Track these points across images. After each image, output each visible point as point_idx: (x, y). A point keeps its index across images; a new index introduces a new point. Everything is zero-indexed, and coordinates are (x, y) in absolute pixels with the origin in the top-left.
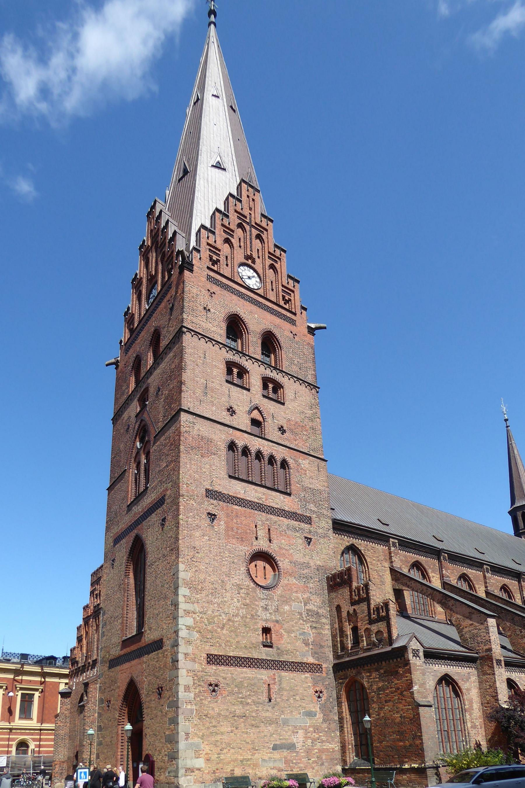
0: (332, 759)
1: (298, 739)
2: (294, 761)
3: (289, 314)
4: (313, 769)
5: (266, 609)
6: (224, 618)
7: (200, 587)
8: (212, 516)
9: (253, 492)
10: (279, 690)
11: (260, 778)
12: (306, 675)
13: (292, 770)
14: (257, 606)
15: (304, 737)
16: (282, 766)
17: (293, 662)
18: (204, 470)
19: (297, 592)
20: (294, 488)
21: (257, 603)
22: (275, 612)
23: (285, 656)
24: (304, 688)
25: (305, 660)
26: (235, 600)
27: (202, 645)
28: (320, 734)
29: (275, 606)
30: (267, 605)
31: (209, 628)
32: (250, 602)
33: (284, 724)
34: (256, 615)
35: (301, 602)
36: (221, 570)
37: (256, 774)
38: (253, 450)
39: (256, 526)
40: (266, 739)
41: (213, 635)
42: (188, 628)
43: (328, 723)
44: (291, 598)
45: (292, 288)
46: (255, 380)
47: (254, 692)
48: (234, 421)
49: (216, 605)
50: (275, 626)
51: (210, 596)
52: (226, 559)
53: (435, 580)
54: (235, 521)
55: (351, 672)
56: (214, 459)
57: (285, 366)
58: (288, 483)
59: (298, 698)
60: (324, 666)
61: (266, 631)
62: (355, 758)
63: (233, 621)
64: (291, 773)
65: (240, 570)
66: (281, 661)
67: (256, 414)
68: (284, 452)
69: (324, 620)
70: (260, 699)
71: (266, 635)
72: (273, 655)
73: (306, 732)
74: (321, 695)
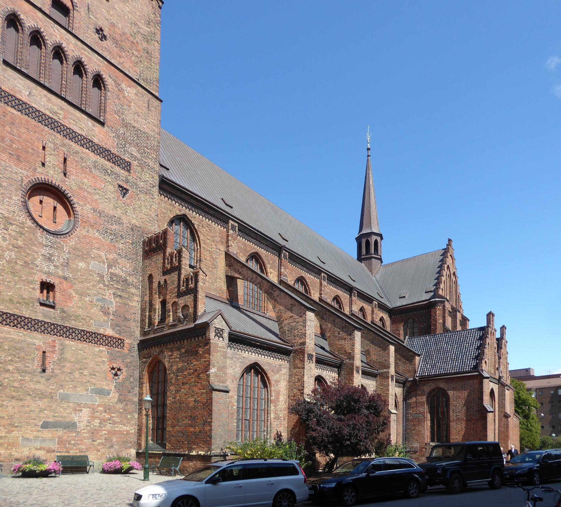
0: (124, 442)
1: (82, 418)
2: (72, 442)
4: (99, 451)
10: (59, 359)
11: (17, 460)
12: (100, 348)
13: (69, 452)
15: (90, 417)
16: (54, 446)
17: (83, 331)
19: (99, 249)
20: (110, 117)
21: (35, 248)
23: (73, 322)
24: (96, 362)
25: (101, 331)
28: (112, 415)
29: (64, 259)
32: (24, 244)
33: (62, 400)
34: (32, 263)
35: (104, 263)
37: (10, 455)
40: (33, 415)
43: (124, 403)
44: (90, 255)
47: (19, 358)
53: (273, 276)
55: (155, 351)
58: (102, 108)
59: (86, 372)
60: (127, 341)
62: (151, 442)
64: (66, 454)
66: (66, 327)
68: (101, 64)
69: (133, 290)
70: (29, 367)
71: (48, 293)
72: (55, 318)
73: (94, 410)
74: (119, 373)
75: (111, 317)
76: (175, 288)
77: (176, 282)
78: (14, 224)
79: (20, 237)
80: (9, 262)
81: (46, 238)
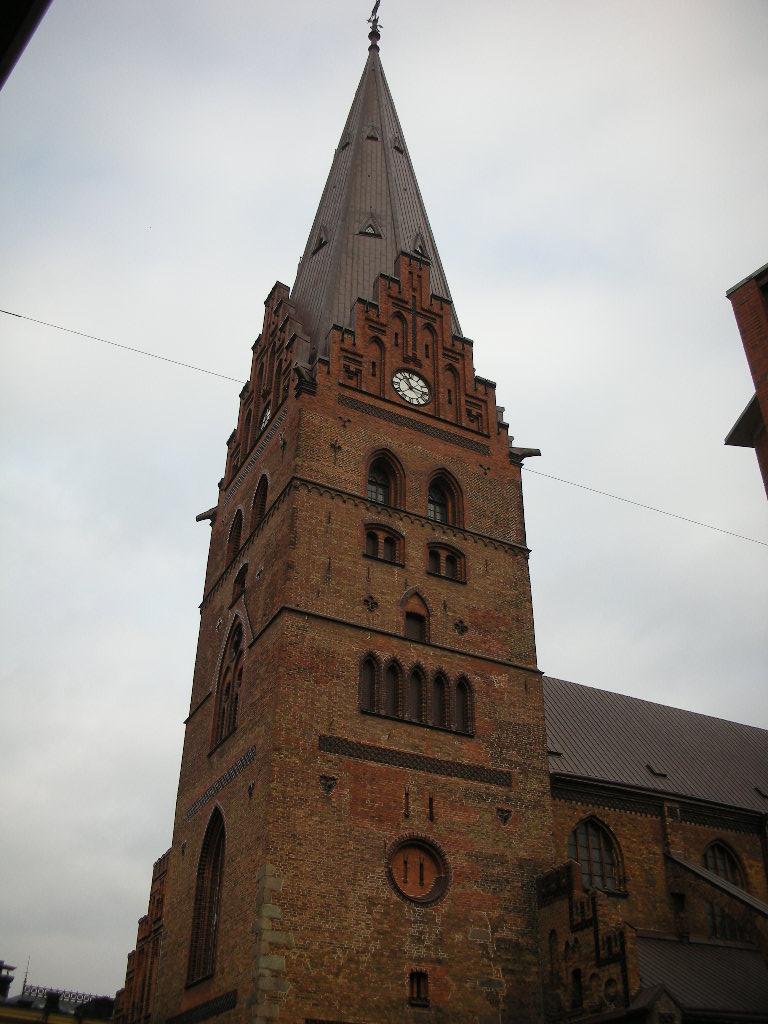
3: (477, 438)
5: (419, 940)
7: (300, 903)
8: (328, 782)
19: (479, 908)
30: (421, 933)
31: (314, 973)
32: (390, 927)
36: (339, 873)
38: (407, 666)
39: (407, 795)
42: (276, 974)
45: (484, 398)
46: (416, 554)
48: (375, 621)
50: (434, 969)
51: (318, 919)
61: (418, 977)
63: (357, 963)
67: (414, 605)
76: (591, 953)
77: (593, 943)
81: (414, 912)
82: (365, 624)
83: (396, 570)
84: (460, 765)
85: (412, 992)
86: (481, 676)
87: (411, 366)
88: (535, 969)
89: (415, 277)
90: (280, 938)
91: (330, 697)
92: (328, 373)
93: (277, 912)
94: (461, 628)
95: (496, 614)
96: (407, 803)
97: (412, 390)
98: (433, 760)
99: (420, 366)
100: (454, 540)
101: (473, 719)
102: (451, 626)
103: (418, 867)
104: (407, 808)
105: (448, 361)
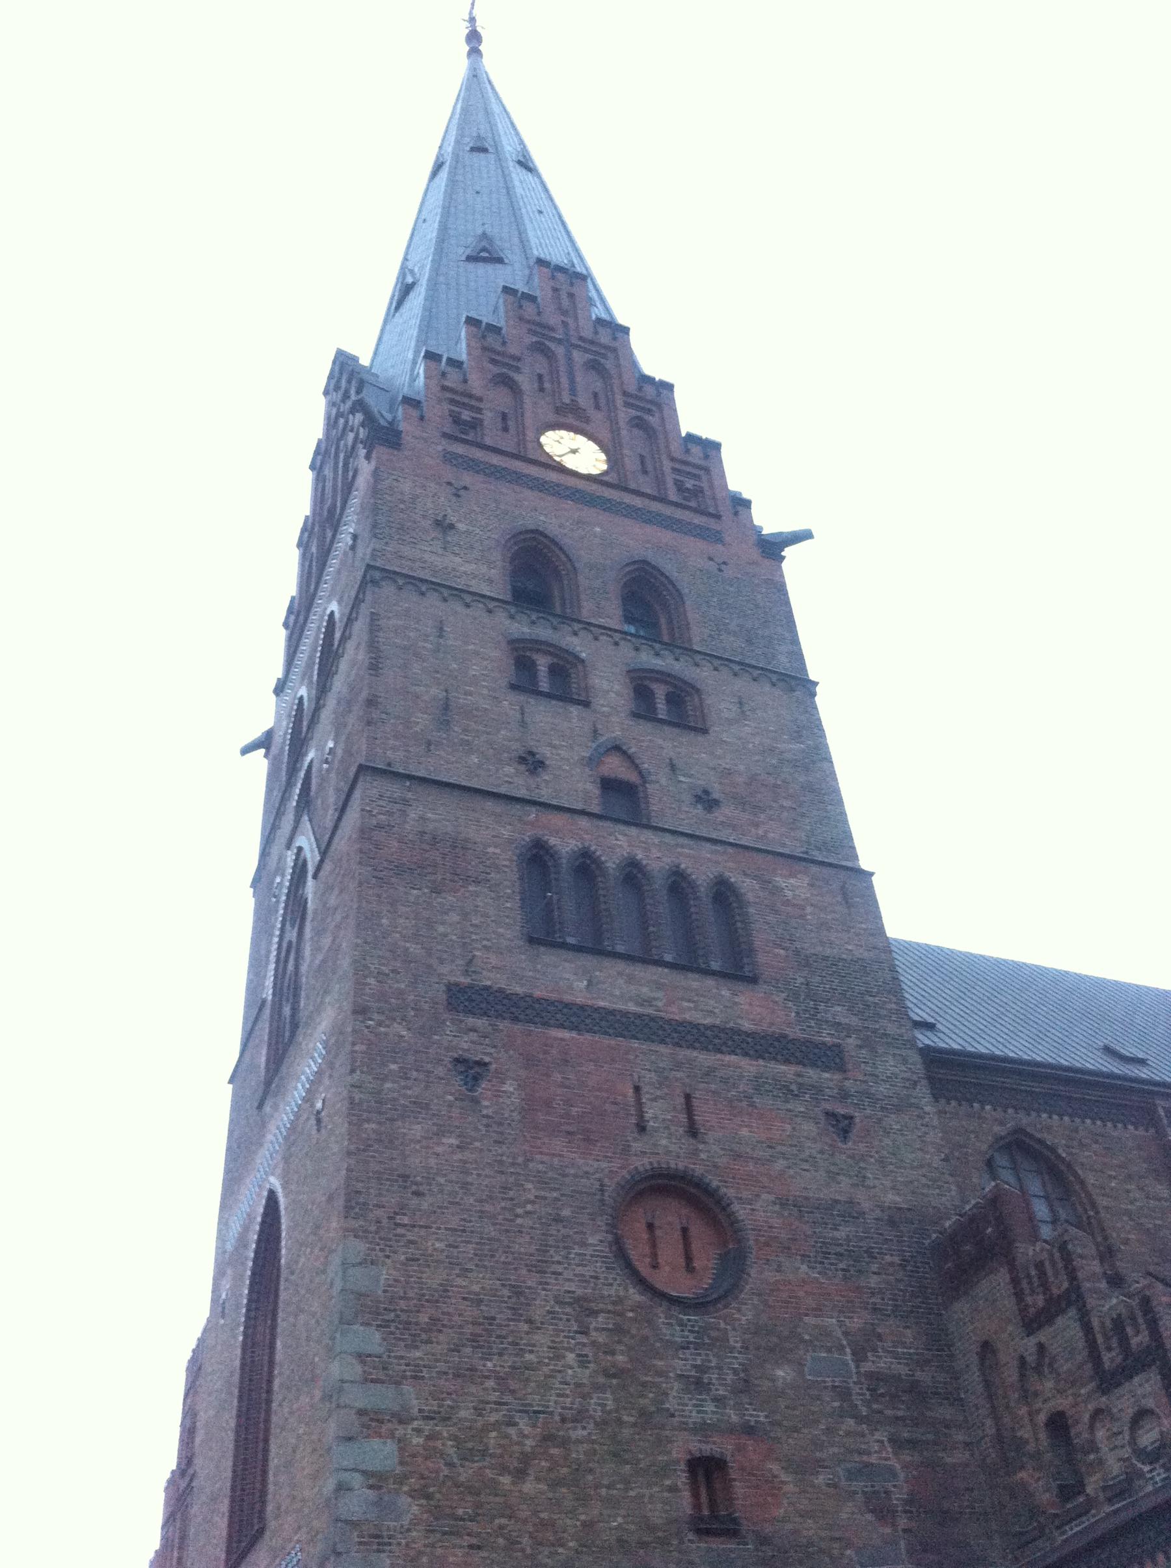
3: (698, 520)
5: (697, 1384)
6: (527, 1430)
7: (424, 1318)
8: (471, 1071)
9: (621, 981)
14: (660, 1373)
18: (441, 929)
19: (818, 1311)
22: (736, 1392)
26: (571, 1357)
27: (433, 1546)
29: (735, 1371)
31: (465, 1474)
34: (659, 1410)
35: (841, 1349)
38: (611, 864)
39: (637, 1089)
41: (479, 1505)
46: (608, 684)
49: (490, 1383)
51: (468, 1350)
52: (529, 1207)
54: (557, 1077)
56: (476, 894)
57: (698, 636)
61: (706, 1470)
63: (565, 1443)
65: (583, 1244)
67: (614, 767)
75: (903, 1522)
78: (602, 1311)
79: (619, 1342)
80: (602, 1424)
82: (522, 793)
83: (574, 710)
84: (739, 1032)
85: (697, 1506)
86: (755, 877)
87: (571, 418)
88: (960, 1437)
89: (564, 296)
90: (383, 1398)
91: (465, 916)
92: (422, 418)
93: (372, 1340)
94: (706, 800)
95: (771, 780)
96: (639, 1104)
97: (578, 453)
98: (681, 1024)
99: (587, 420)
100: (679, 667)
101: (751, 951)
102: (687, 798)
103: (677, 1234)
104: (641, 1114)
105: (634, 413)
